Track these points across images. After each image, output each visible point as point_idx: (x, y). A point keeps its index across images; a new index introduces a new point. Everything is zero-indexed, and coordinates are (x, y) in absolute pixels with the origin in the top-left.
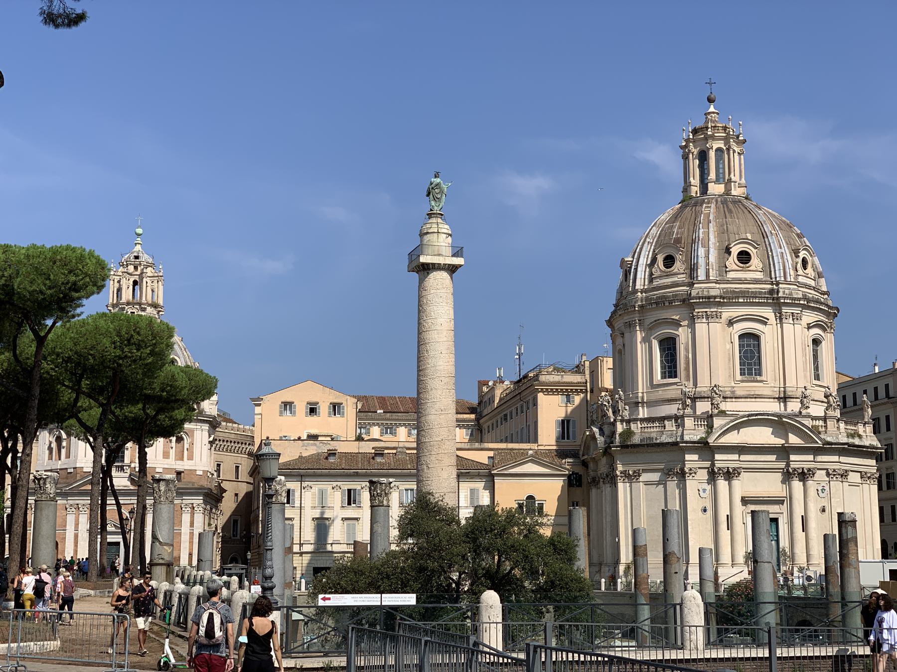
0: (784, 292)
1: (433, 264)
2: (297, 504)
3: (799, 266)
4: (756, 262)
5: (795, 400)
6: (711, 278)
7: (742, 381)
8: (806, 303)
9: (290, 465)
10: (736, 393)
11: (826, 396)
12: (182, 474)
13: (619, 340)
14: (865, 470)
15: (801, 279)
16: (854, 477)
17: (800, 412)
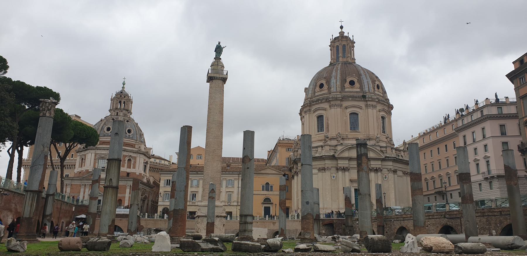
0: (368, 96)
1: (214, 77)
3: (376, 87)
4: (357, 85)
5: (373, 140)
6: (338, 91)
7: (351, 132)
8: (378, 101)
12: (130, 174)
14: (405, 170)
15: (376, 92)
16: (400, 173)
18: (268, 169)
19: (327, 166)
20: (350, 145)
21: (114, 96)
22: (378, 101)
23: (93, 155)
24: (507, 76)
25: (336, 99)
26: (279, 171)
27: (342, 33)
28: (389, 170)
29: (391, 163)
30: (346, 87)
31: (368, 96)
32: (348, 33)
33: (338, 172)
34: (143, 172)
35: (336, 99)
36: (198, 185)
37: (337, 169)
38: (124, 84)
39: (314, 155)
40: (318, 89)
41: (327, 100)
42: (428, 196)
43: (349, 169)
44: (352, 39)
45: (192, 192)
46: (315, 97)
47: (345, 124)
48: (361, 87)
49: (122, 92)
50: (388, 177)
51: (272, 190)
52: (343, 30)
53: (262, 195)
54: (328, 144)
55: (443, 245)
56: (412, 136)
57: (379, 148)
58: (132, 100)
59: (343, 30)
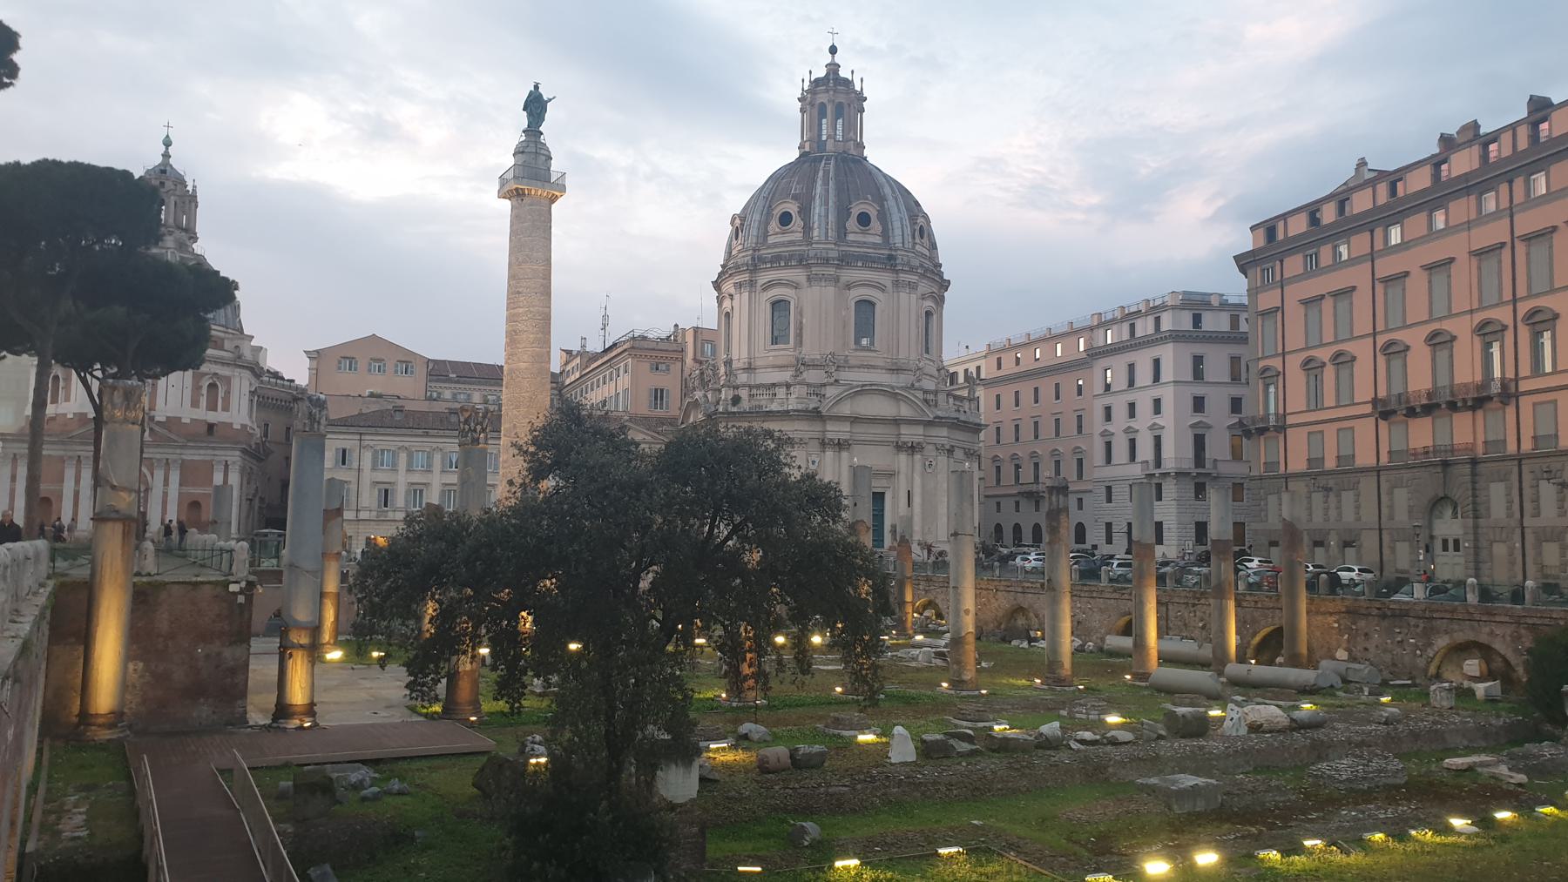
0: (902, 259)
2: (355, 465)
3: (917, 233)
4: (876, 225)
9: (346, 421)
10: (850, 362)
11: (938, 370)
13: (727, 304)
17: (913, 385)
19: (796, 436)
20: (858, 386)
24: (1234, 257)
25: (826, 261)
26: (656, 435)
27: (833, 68)
29: (944, 432)
31: (902, 259)
32: (853, 72)
33: (824, 452)
35: (826, 261)
36: (430, 465)
37: (823, 444)
38: (167, 143)
39: (766, 407)
40: (774, 225)
41: (801, 261)
42: (998, 499)
43: (850, 445)
45: (413, 484)
46: (769, 247)
47: (844, 327)
48: (885, 234)
49: (164, 172)
50: (937, 464)
52: (838, 59)
54: (804, 379)
55: (1278, 719)
56: (967, 347)
57: (920, 395)
59: (838, 59)
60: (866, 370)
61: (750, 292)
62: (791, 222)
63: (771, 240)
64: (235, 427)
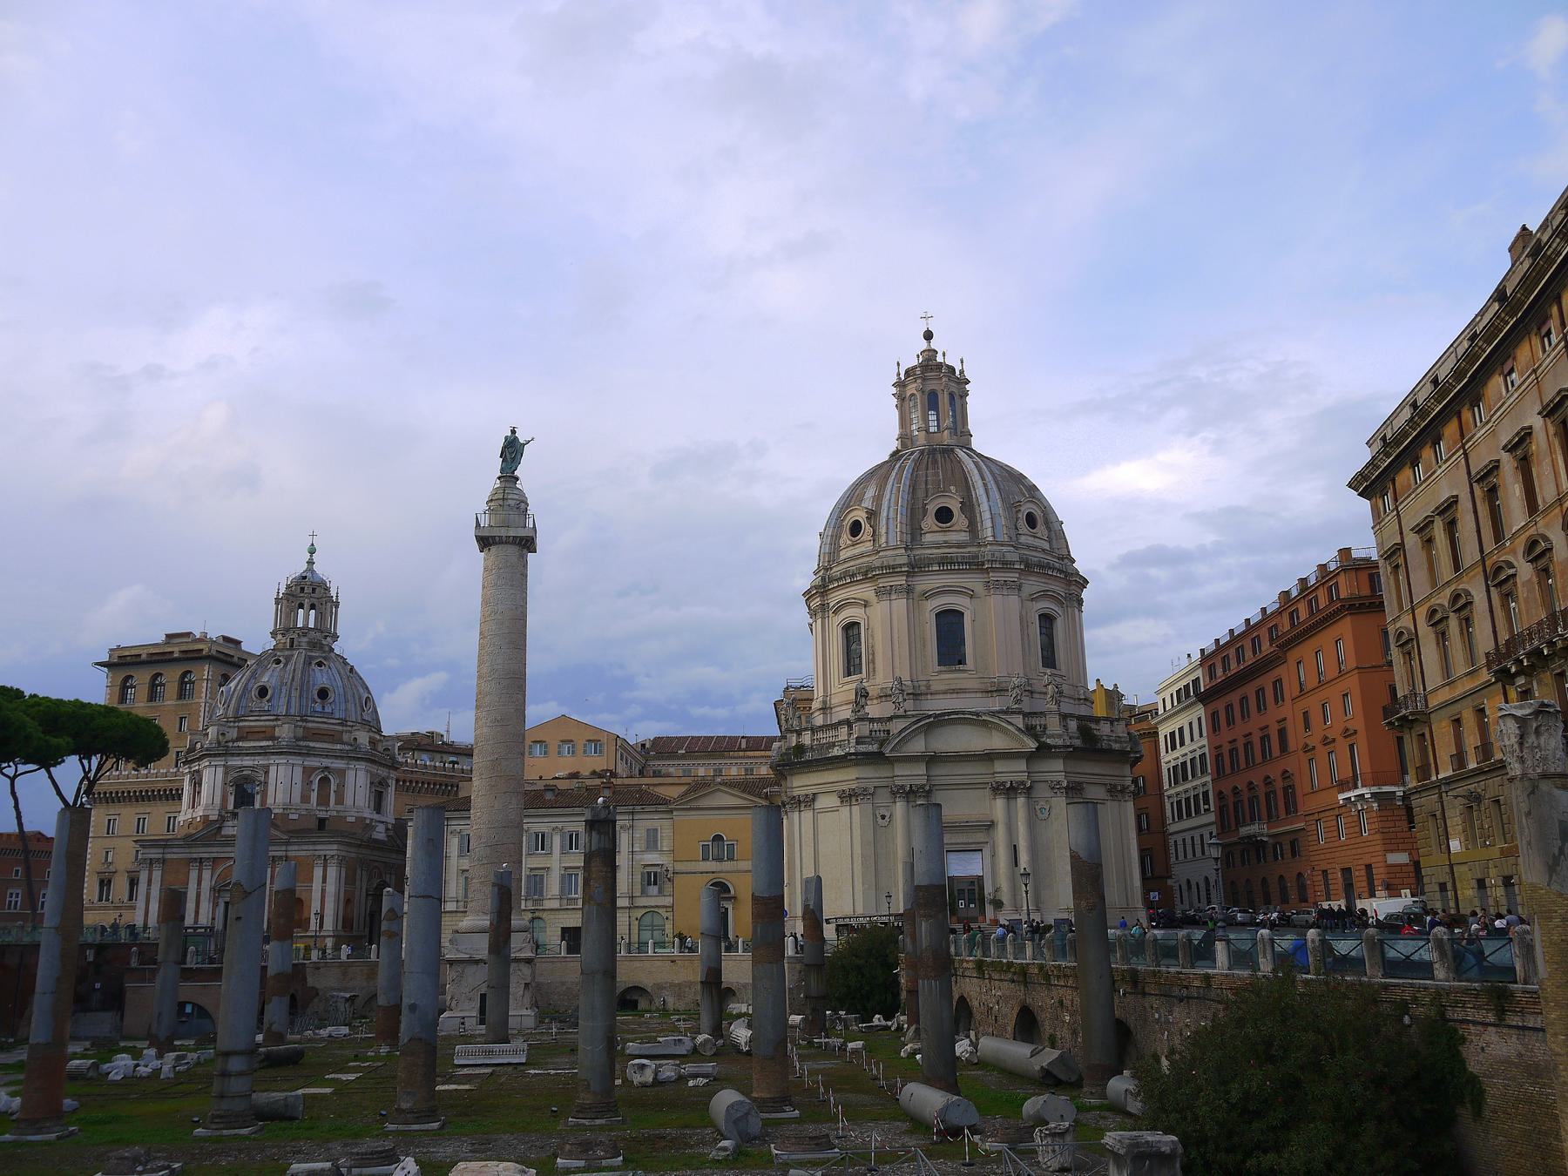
0: (993, 555)
3: (1022, 523)
4: (960, 520)
7: (940, 672)
8: (1022, 567)
12: (327, 822)
15: (1023, 539)
18: (719, 794)
20: (930, 716)
21: (283, 590)
22: (1022, 567)
23: (220, 771)
24: (1350, 485)
28: (1054, 787)
29: (1058, 765)
30: (926, 530)
31: (993, 555)
34: (368, 814)
35: (892, 570)
38: (312, 551)
40: (846, 538)
44: (958, 369)
46: (839, 564)
48: (973, 528)
49: (305, 578)
51: (731, 859)
52: (934, 344)
53: (702, 873)
56: (1189, 655)
57: (1019, 721)
58: (337, 596)
59: (934, 344)
60: (955, 696)
61: (823, 618)
62: (861, 528)
63: (843, 555)
64: (350, 819)
